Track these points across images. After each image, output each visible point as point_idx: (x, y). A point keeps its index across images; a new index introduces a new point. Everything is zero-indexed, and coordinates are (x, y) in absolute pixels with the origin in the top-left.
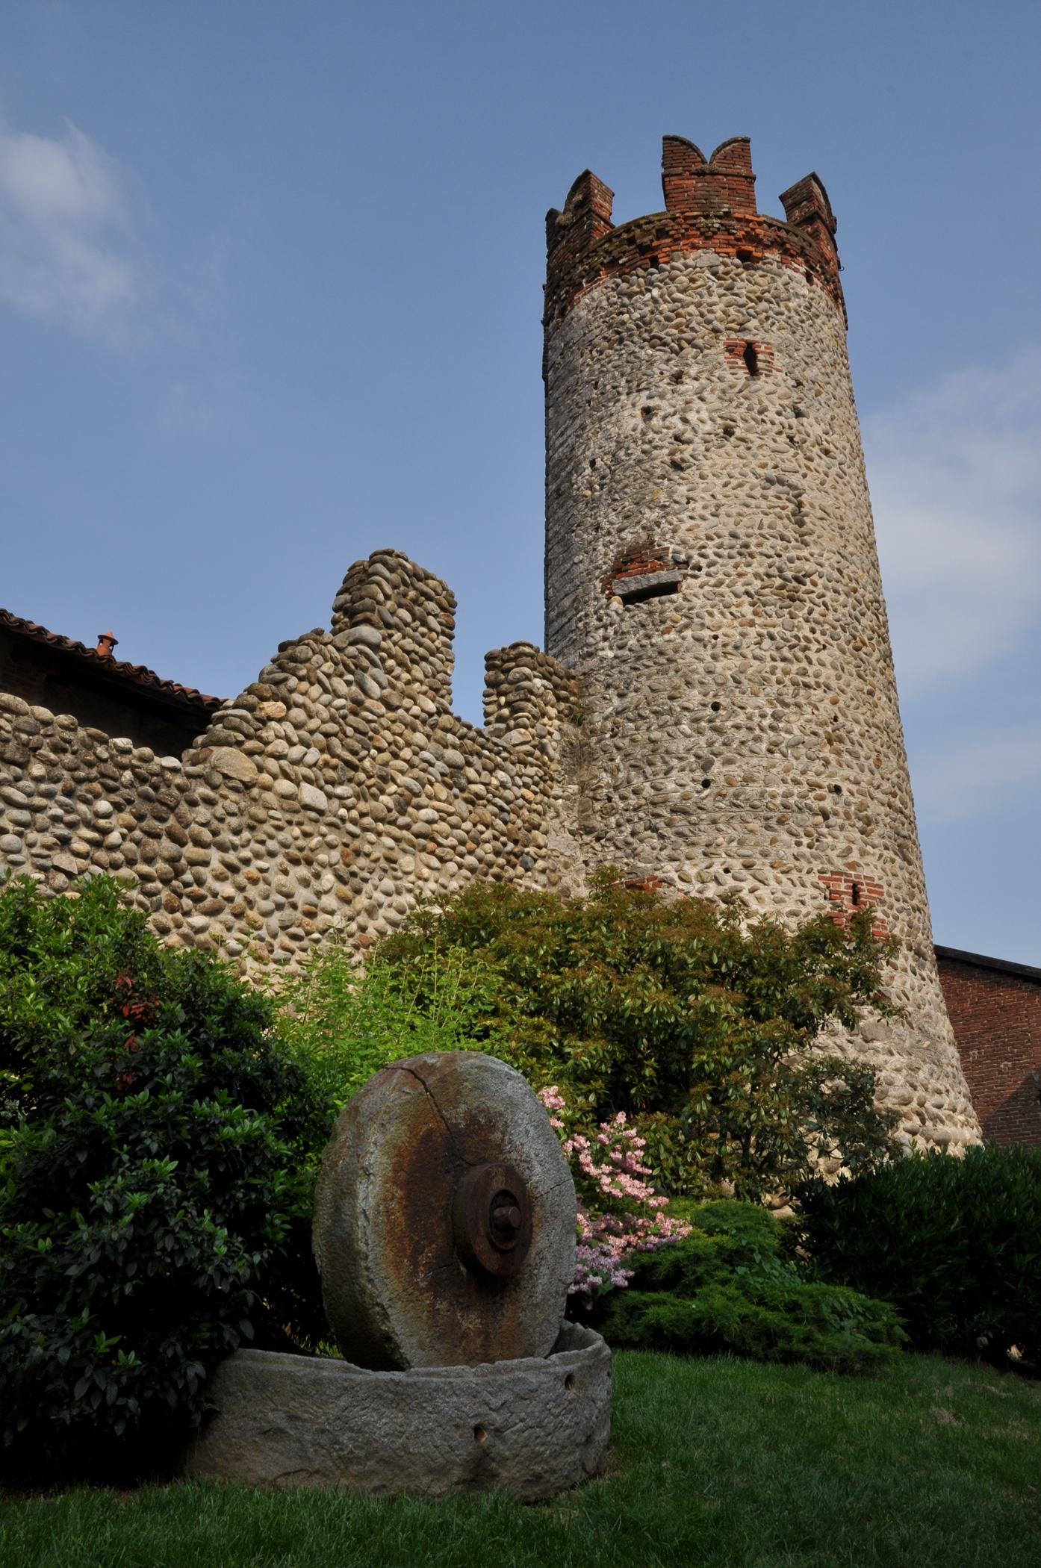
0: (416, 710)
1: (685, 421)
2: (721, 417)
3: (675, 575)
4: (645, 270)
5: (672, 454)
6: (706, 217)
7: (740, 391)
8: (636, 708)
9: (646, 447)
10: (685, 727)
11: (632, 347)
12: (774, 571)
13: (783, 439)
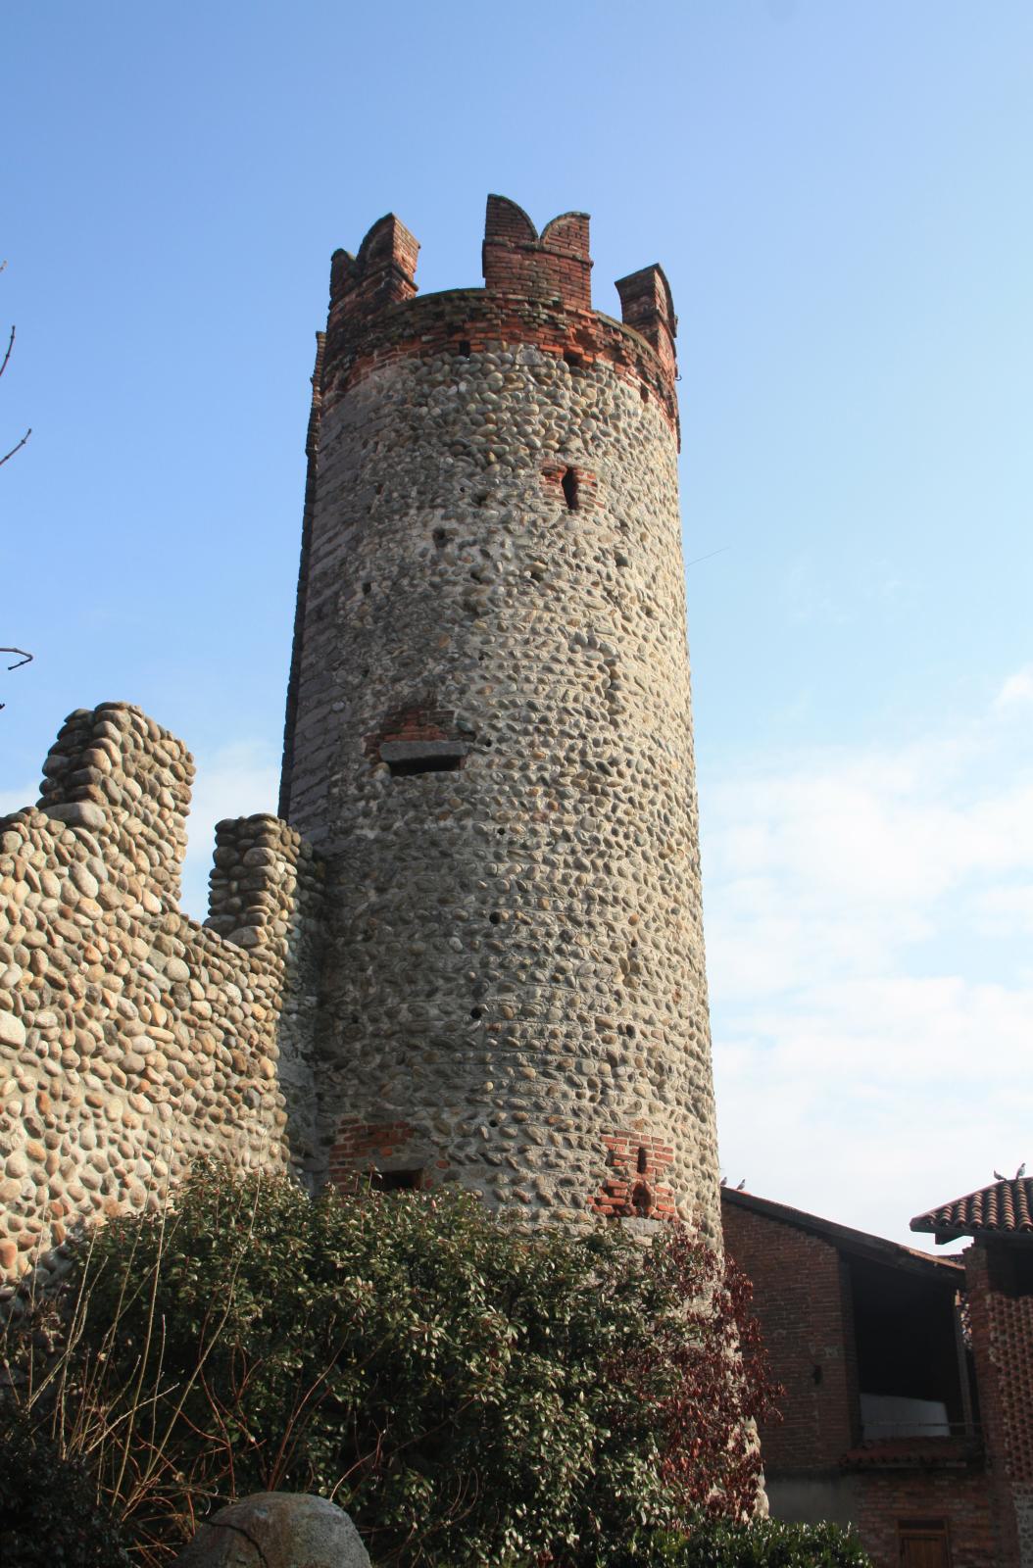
0: (138, 910)
1: (486, 554)
4: (453, 356)
5: (467, 593)
6: (531, 304)
8: (398, 909)
9: (437, 579)
10: (456, 941)
11: (429, 451)
12: (575, 756)
13: (598, 592)
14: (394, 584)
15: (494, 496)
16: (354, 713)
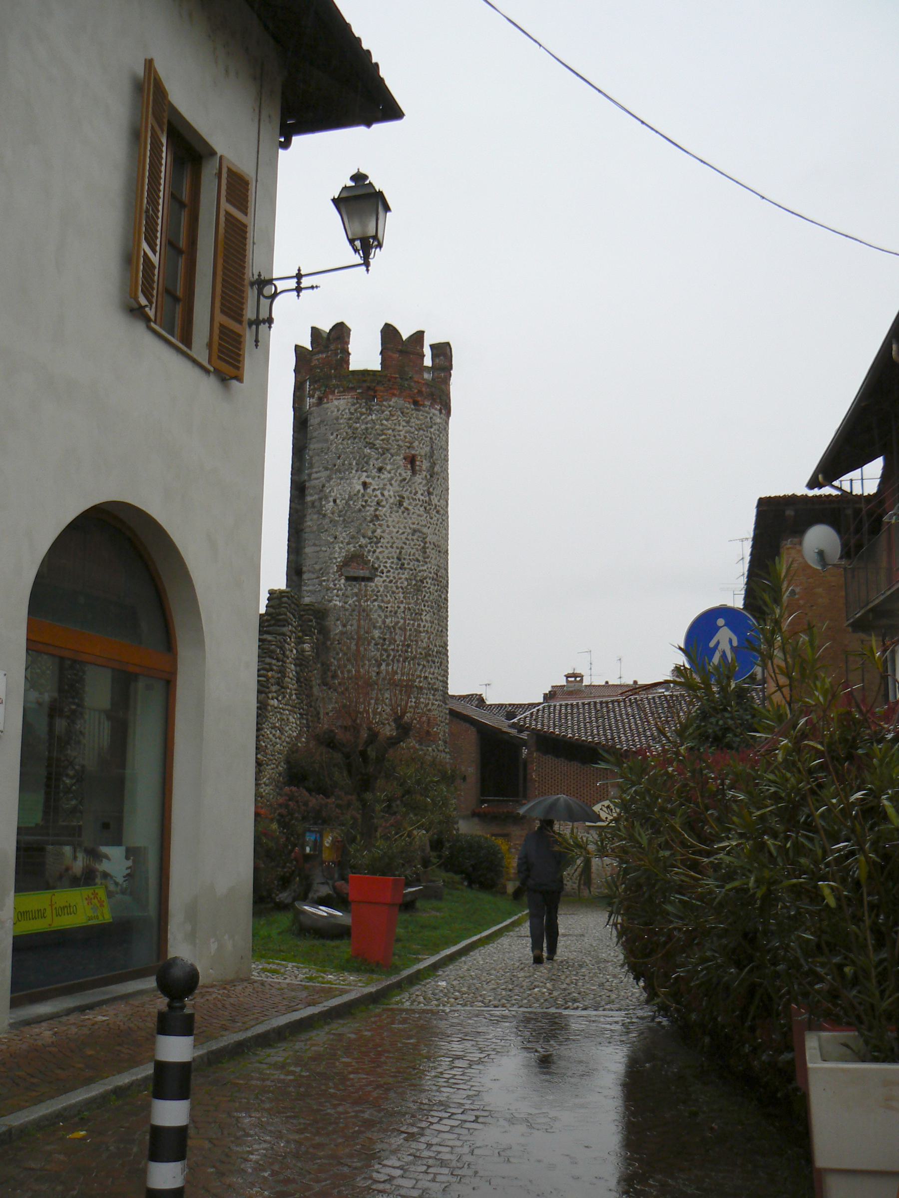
2: (398, 496)
7: (408, 483)
9: (364, 504)
12: (413, 577)
14: (347, 502)
15: (385, 469)
16: (331, 554)
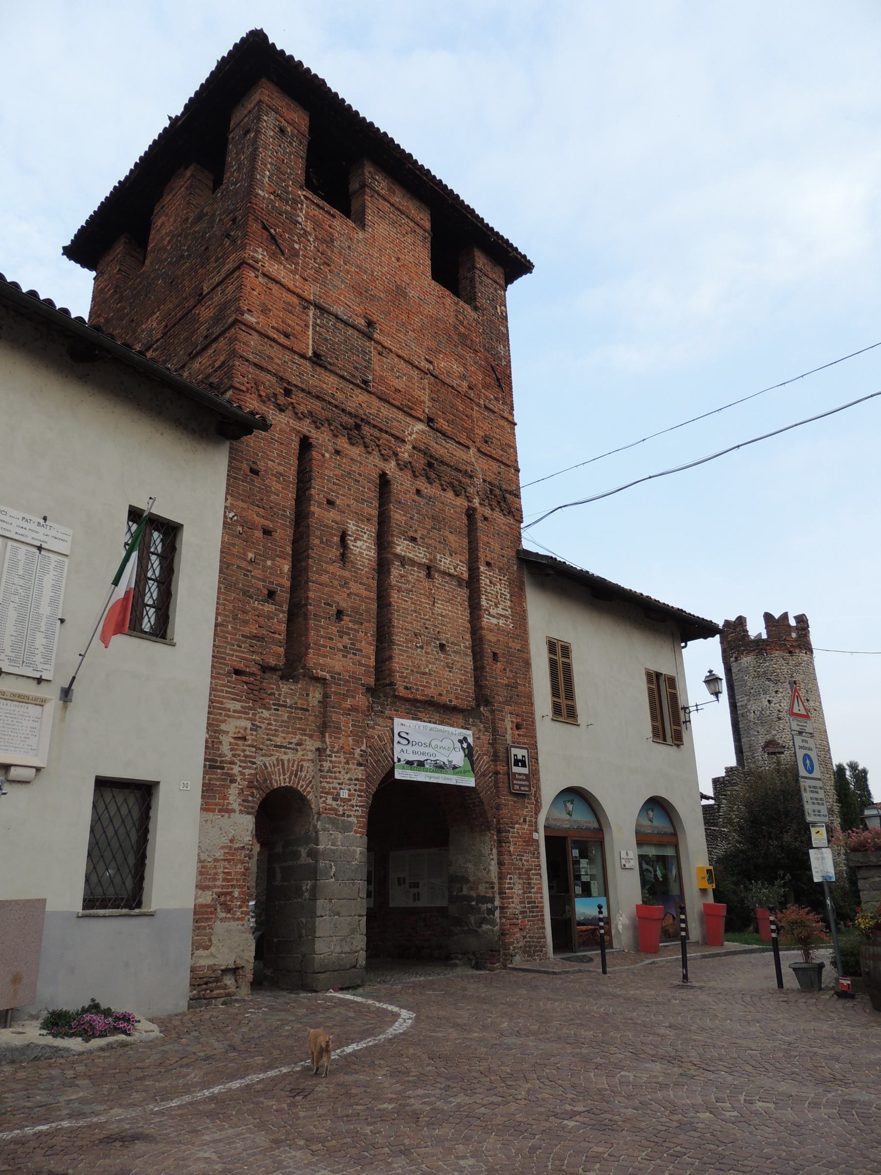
3: (782, 750)
